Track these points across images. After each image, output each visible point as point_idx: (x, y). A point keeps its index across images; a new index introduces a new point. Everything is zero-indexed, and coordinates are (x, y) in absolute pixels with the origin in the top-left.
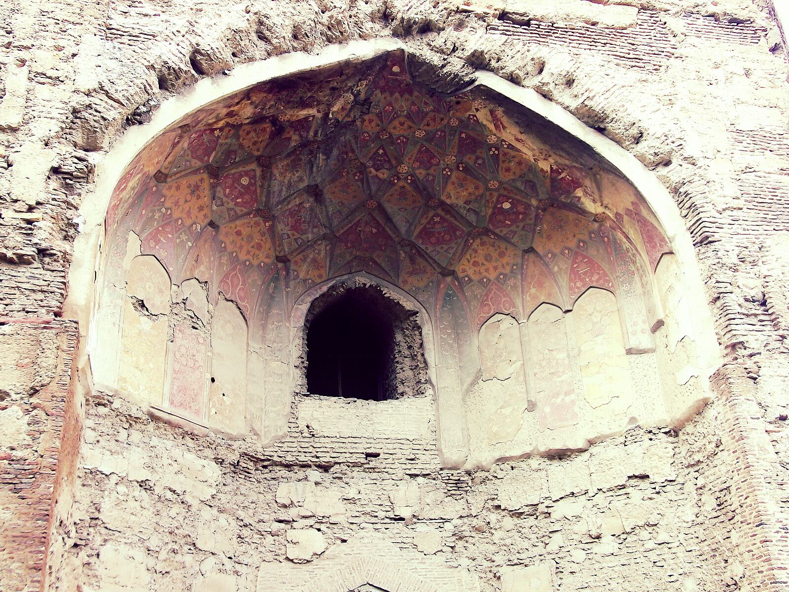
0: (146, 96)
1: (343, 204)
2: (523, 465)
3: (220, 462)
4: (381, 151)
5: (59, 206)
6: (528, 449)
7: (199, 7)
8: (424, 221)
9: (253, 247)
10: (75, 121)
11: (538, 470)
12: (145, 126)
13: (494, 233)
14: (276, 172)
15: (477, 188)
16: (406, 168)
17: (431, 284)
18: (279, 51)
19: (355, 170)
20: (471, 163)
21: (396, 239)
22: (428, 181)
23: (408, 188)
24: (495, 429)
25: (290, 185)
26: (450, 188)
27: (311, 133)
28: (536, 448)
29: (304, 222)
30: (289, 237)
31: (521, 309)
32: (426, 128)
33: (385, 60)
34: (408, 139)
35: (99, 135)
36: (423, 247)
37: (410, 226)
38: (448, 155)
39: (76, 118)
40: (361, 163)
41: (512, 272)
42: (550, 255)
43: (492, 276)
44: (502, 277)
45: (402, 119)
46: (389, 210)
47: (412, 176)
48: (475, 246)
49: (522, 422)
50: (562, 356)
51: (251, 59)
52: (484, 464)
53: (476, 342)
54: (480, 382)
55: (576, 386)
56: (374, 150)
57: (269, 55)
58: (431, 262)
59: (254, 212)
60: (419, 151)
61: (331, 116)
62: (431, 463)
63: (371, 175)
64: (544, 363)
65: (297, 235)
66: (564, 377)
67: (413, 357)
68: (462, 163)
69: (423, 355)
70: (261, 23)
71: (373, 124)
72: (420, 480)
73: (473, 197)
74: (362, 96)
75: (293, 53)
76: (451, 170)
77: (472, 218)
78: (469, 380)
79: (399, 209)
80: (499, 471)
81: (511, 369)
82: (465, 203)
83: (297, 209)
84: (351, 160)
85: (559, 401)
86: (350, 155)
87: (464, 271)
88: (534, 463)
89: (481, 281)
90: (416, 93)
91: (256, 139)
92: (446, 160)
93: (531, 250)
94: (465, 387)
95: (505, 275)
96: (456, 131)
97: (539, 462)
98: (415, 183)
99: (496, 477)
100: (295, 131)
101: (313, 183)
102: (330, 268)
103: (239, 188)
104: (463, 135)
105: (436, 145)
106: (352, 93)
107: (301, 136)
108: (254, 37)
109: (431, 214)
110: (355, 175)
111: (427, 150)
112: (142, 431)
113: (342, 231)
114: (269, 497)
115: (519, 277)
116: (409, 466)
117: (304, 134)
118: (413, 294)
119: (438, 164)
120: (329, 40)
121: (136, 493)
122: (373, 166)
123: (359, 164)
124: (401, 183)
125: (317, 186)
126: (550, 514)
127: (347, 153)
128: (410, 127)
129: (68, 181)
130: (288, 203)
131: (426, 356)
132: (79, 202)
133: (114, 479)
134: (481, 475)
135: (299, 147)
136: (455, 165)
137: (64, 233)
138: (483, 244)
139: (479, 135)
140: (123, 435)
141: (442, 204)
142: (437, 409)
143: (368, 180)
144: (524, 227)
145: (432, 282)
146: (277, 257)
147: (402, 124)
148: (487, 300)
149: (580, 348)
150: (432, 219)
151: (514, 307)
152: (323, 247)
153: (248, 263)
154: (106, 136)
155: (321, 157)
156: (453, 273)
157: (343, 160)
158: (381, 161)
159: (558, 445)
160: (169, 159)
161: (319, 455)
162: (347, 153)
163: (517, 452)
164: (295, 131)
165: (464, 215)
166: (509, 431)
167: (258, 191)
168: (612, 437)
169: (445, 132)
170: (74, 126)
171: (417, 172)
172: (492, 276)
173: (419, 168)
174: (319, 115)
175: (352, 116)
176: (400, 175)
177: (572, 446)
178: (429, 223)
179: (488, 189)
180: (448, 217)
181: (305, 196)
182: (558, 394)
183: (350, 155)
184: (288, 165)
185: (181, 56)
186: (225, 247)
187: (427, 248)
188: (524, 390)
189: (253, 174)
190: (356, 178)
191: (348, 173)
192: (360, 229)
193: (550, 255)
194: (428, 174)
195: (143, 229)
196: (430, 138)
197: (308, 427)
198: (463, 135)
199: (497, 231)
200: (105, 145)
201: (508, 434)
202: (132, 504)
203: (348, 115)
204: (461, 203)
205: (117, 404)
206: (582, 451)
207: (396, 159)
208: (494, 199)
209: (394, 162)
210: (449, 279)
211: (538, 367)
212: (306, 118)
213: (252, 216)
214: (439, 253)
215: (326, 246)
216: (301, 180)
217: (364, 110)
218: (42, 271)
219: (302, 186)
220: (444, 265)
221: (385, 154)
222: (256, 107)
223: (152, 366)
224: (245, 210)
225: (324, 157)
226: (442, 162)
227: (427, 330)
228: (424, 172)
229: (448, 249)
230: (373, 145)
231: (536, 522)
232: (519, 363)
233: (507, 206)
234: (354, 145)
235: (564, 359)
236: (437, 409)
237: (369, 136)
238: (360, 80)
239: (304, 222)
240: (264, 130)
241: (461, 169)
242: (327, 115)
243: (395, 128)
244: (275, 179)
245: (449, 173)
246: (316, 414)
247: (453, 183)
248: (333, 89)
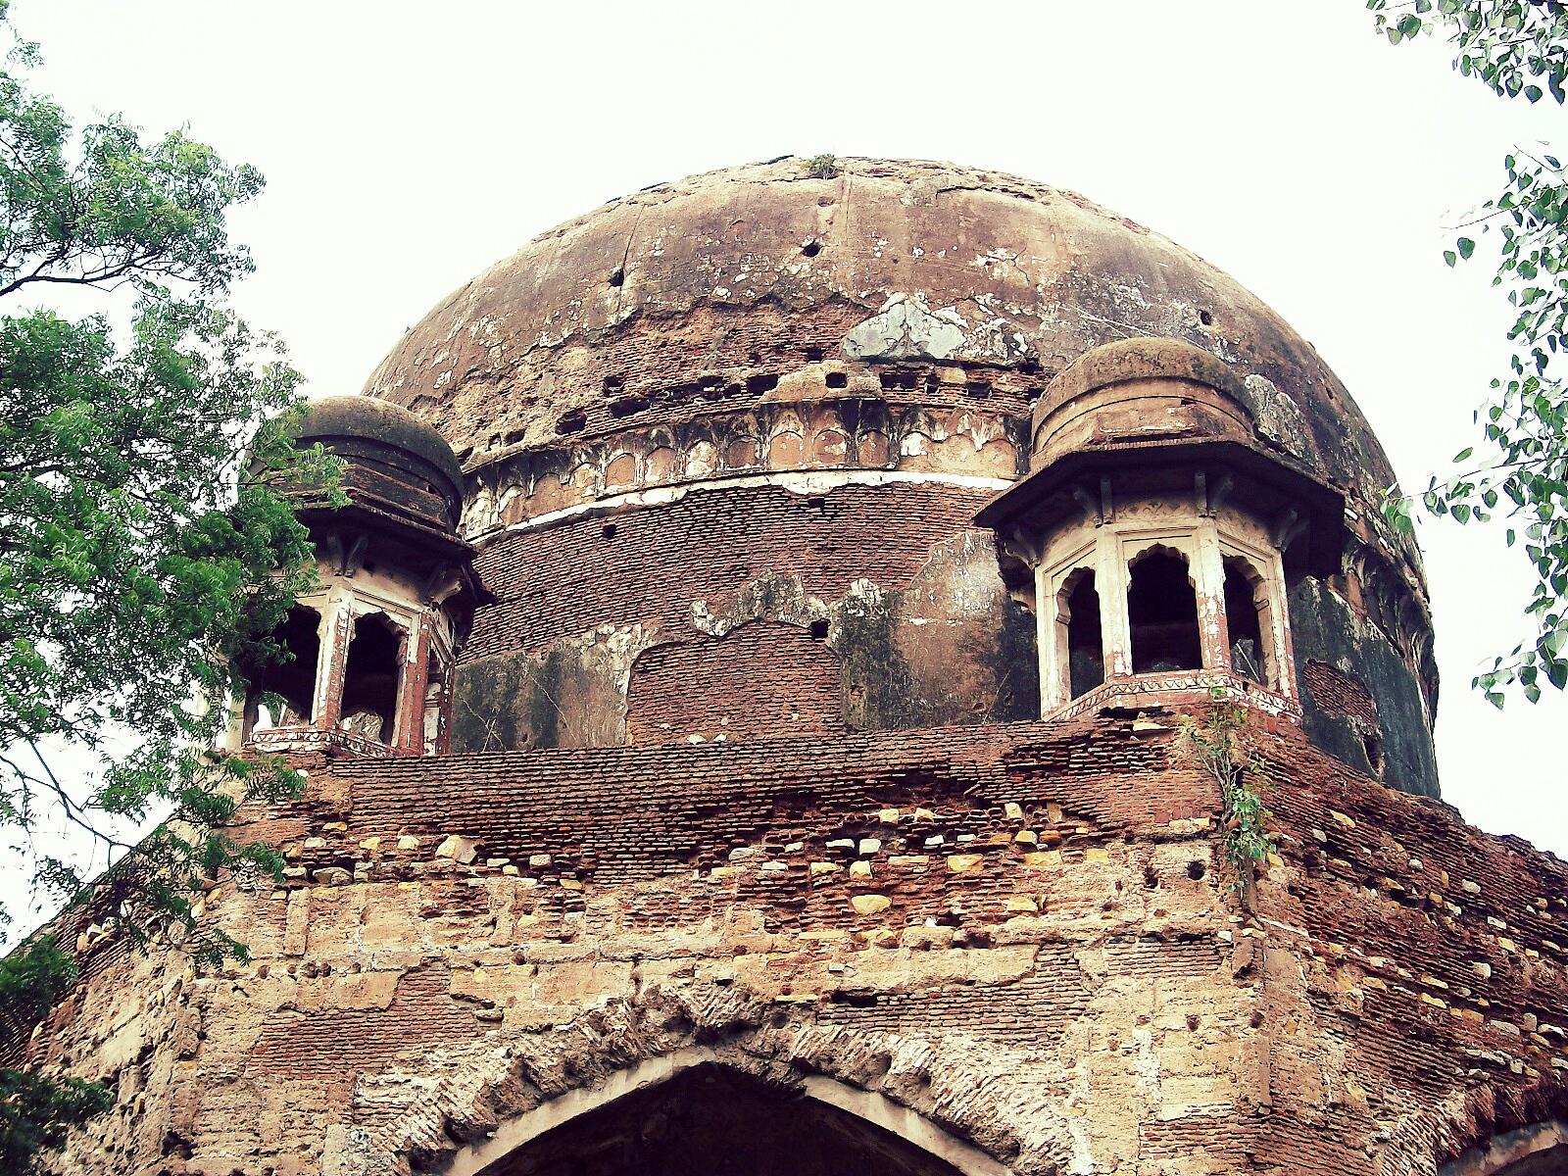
18: (552, 1097)
33: (684, 1076)
51: (519, 1114)
57: (540, 1102)
75: (570, 1093)
108: (519, 1084)
120: (616, 1067)
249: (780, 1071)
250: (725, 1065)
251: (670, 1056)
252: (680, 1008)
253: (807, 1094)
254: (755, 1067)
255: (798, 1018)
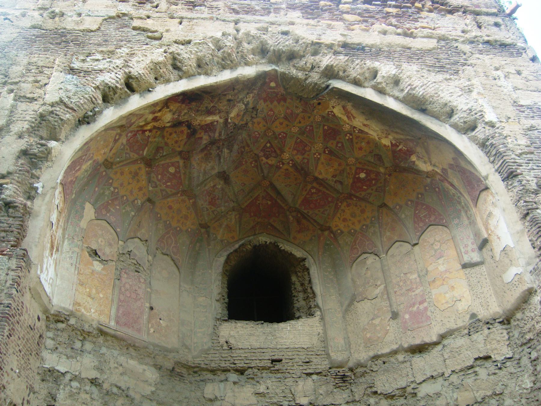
0: (93, 105)
1: (245, 184)
2: (392, 359)
3: (159, 368)
4: (268, 145)
5: (24, 174)
6: (395, 347)
7: (133, 52)
8: (305, 193)
9: (182, 217)
10: (42, 122)
11: (403, 362)
12: (92, 125)
13: (356, 197)
14: (194, 163)
15: (340, 165)
16: (287, 155)
17: (313, 238)
19: (251, 160)
20: (334, 147)
21: (285, 208)
22: (304, 163)
23: (291, 170)
24: (368, 336)
25: (205, 173)
26: (320, 167)
27: (217, 135)
28: (401, 345)
29: (218, 199)
30: (207, 210)
31: (381, 249)
32: (299, 125)
33: (262, 77)
34: (286, 134)
35: (58, 130)
36: (306, 211)
37: (294, 198)
38: (316, 143)
39: (43, 120)
40: (256, 154)
41: (371, 223)
42: (398, 207)
43: (358, 227)
44: (364, 227)
45: (282, 121)
46: (278, 187)
47: (292, 160)
48: (342, 207)
49: (388, 328)
50: (414, 276)
52: (362, 361)
53: (350, 276)
54: (355, 303)
55: (427, 297)
56: (264, 144)
58: (312, 221)
59: (180, 192)
60: (296, 142)
61: (229, 121)
62: (323, 365)
63: (263, 162)
64: (401, 284)
65: (214, 208)
66: (417, 292)
67: (305, 291)
68: (327, 148)
69: (311, 288)
70: (174, 59)
71: (261, 125)
72: (315, 377)
73: (338, 172)
74: (251, 106)
75: (198, 76)
76: (320, 154)
77: (339, 187)
78: (346, 303)
79: (286, 186)
80: (374, 366)
81: (377, 291)
82: (333, 177)
83: (212, 189)
84: (247, 153)
85: (415, 309)
86: (246, 148)
87: (337, 226)
88: (400, 357)
89: (349, 232)
90: (289, 100)
91: (177, 139)
92: (316, 147)
93: (384, 205)
94: (344, 308)
95: (367, 226)
96: (320, 125)
97: (403, 356)
98: (294, 165)
99: (372, 370)
100: (205, 132)
101: (222, 170)
102: (239, 233)
103: (168, 175)
104: (326, 128)
105: (307, 136)
106: (243, 103)
107: (210, 136)
109: (309, 186)
110: (251, 163)
111: (301, 141)
112: (94, 343)
113: (246, 204)
114: (199, 394)
115: (377, 225)
116: (305, 367)
117: (212, 134)
118: (301, 246)
119: (310, 150)
121: (88, 388)
122: (264, 155)
123: (253, 155)
124: (285, 167)
125: (224, 172)
126: (416, 394)
127: (244, 147)
128: (287, 126)
129: (33, 160)
130: (205, 186)
131: (314, 288)
132: (39, 173)
133: (68, 377)
134: (360, 370)
135: (209, 144)
136: (323, 150)
137: (28, 194)
138: (348, 206)
139: (336, 126)
140: (78, 345)
141: (316, 179)
142: (324, 325)
143: (261, 166)
144: (376, 189)
145: (314, 236)
146: (200, 225)
147: (281, 124)
148: (355, 244)
149: (427, 269)
150: (310, 190)
151: (376, 247)
152: (233, 217)
153: (178, 229)
154: (63, 131)
155: (226, 151)
156: (329, 229)
157: (242, 153)
158: (269, 151)
159: (418, 342)
160: (113, 151)
161: (236, 362)
162: (244, 147)
163: (386, 350)
164: (205, 132)
165: (333, 185)
166: (379, 335)
167: (182, 177)
168: (458, 330)
169: (312, 126)
170: (40, 125)
171: (296, 157)
172: (358, 227)
173: (297, 154)
174: (221, 121)
175: (245, 120)
176: (284, 161)
177: (427, 340)
178: (308, 194)
179: (347, 165)
180: (321, 188)
181: (217, 180)
182: (414, 304)
183: (246, 148)
184: (202, 158)
185: (118, 79)
186: (160, 217)
187: (308, 212)
188: (388, 304)
189: (177, 164)
190: (253, 165)
191: (246, 162)
192: (259, 202)
193: (398, 207)
194: (304, 158)
195: (96, 201)
196: (302, 132)
197: (227, 342)
198: (326, 128)
199: (357, 194)
200: (62, 136)
201: (379, 338)
202: (83, 396)
203: (242, 120)
204: (329, 177)
205: (72, 321)
206: (436, 344)
207: (280, 149)
208: (353, 172)
209: (278, 152)
210: (326, 233)
211: (397, 286)
212: (212, 123)
213: (179, 195)
214: (317, 215)
215: (235, 216)
216: (213, 168)
217: (254, 116)
218: (7, 218)
219: (214, 172)
220: (322, 223)
221: (271, 146)
222: (174, 114)
223: (101, 296)
224: (174, 191)
225: (228, 151)
226: (313, 148)
227: (314, 271)
228: (301, 157)
229: (324, 211)
230: (262, 141)
231: (405, 401)
232: (382, 287)
233: (363, 175)
234: (249, 142)
235: (415, 279)
236: (324, 325)
237: (259, 134)
238: (248, 93)
239: (218, 199)
240: (182, 132)
241: (327, 152)
242: (227, 120)
243: (276, 127)
244: (194, 168)
245: (319, 156)
246: (232, 333)
247: (323, 163)
248: (229, 100)
249: (315, 77)
250: (284, 74)
251: (254, 66)
252: (261, 42)
253: (330, 87)
254: (300, 75)
255: (326, 51)
